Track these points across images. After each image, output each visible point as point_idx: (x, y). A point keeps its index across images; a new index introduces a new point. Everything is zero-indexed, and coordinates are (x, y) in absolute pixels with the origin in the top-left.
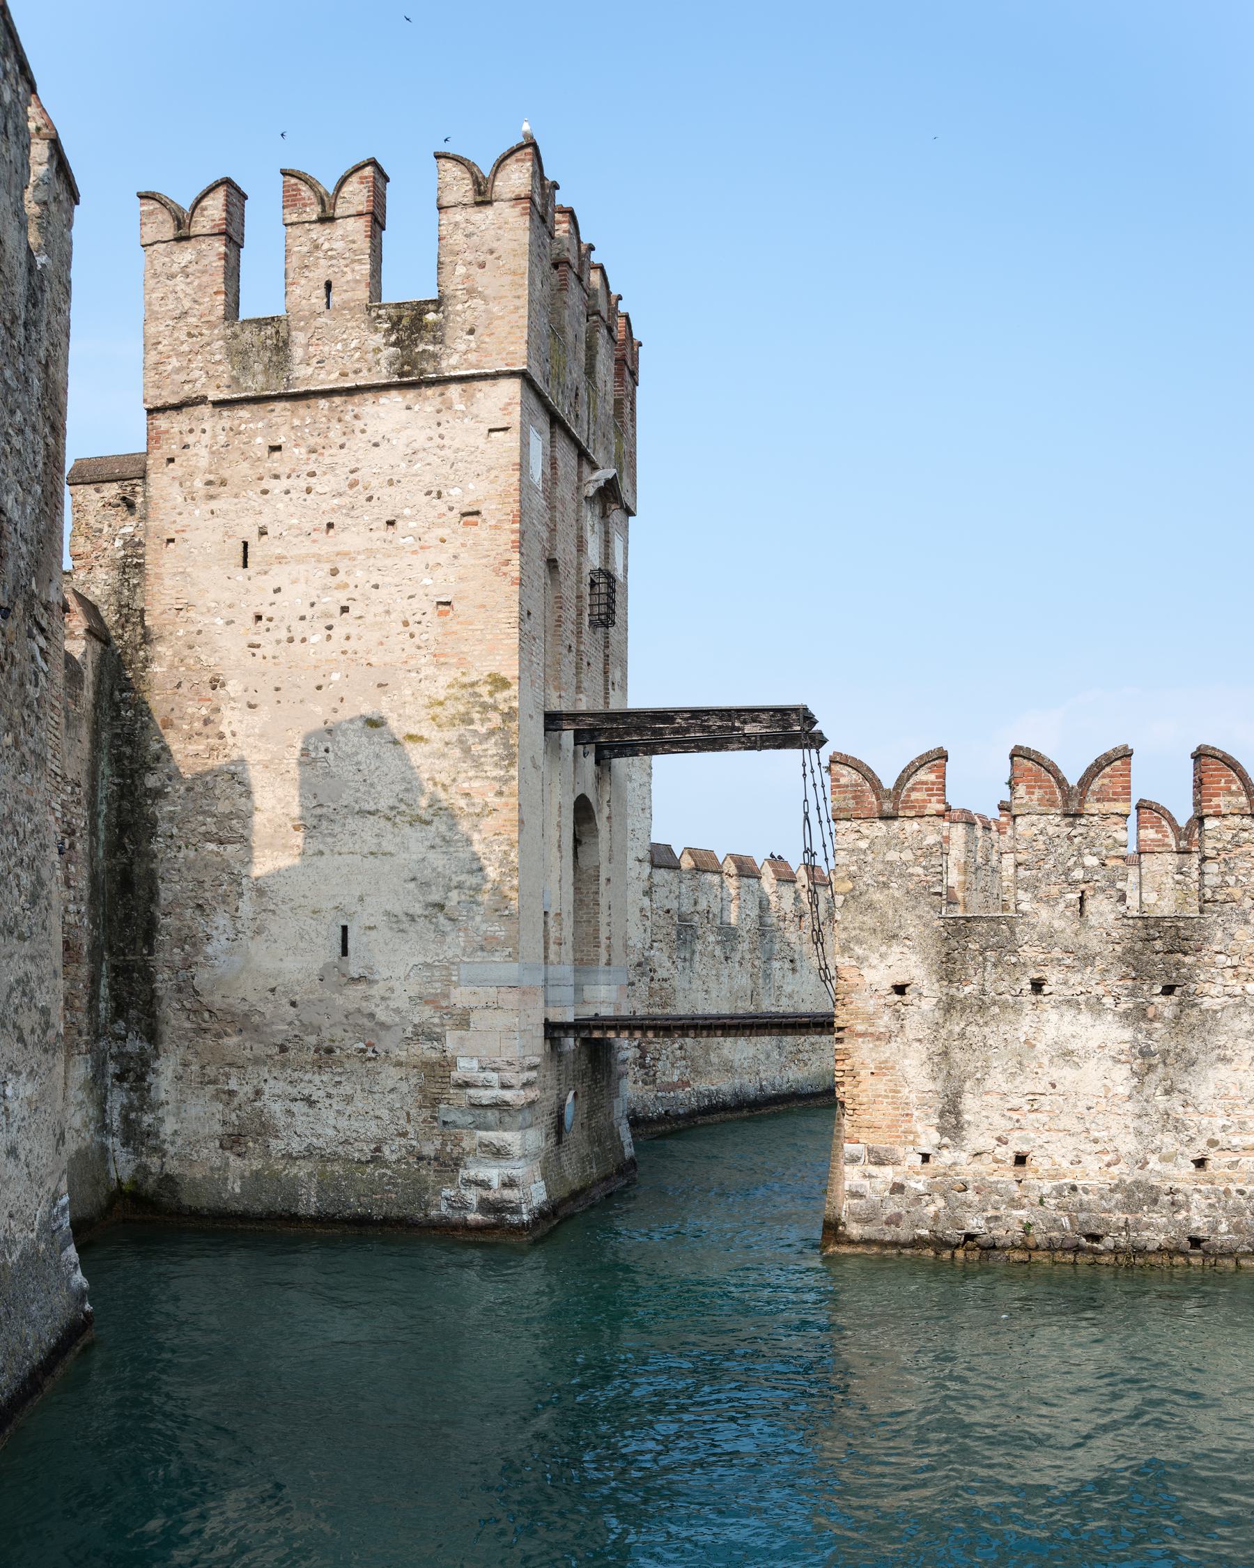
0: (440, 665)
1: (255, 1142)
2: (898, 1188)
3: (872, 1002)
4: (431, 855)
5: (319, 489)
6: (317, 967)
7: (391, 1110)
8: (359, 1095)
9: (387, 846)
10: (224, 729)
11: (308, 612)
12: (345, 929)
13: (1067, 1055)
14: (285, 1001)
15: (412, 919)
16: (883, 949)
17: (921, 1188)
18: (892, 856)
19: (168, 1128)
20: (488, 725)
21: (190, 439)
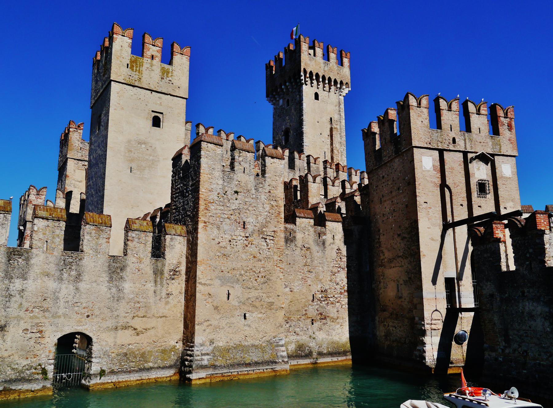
0: (407, 219)
1: (389, 337)
2: (496, 359)
3: (485, 300)
4: (409, 266)
5: (390, 183)
6: (395, 294)
7: (406, 330)
8: (402, 326)
9: (403, 264)
10: (381, 240)
11: (389, 212)
12: (398, 285)
13: (531, 316)
14: (391, 303)
15: (406, 281)
16: (486, 283)
17: (501, 359)
18: (485, 255)
19: (378, 333)
20: (415, 232)
21: (373, 178)
